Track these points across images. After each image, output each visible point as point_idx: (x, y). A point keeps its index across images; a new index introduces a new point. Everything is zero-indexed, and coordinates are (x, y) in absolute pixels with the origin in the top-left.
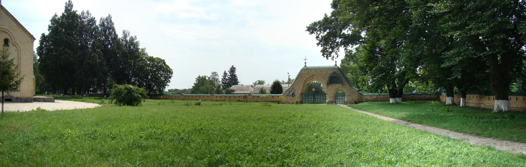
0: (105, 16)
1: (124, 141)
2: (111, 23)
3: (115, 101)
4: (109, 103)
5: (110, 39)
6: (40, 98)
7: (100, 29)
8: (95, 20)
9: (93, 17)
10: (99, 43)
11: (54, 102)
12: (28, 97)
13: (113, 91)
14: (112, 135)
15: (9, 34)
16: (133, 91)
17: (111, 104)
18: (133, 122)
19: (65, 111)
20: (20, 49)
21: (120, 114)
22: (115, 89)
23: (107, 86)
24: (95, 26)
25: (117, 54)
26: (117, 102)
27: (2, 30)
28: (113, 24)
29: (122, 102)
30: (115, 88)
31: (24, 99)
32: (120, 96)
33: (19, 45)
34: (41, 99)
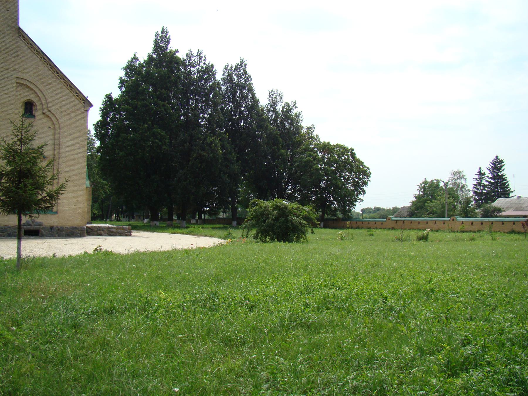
0: (234, 62)
1: (272, 313)
2: (245, 77)
3: (254, 232)
4: (242, 236)
5: (243, 109)
6: (101, 227)
7: (223, 88)
8: (214, 70)
9: (210, 65)
10: (222, 117)
11: (130, 235)
12: (75, 226)
13: (250, 212)
14: (249, 302)
15: (36, 93)
16: (291, 212)
17: (246, 240)
18: (289, 274)
19: (153, 254)
20: (58, 123)
21: (265, 259)
22: (254, 209)
23: (238, 202)
24: (213, 81)
25: (258, 139)
26: (258, 234)
27: (20, 81)
28: (249, 78)
29: (268, 234)
30: (254, 207)
31: (67, 229)
32: (264, 221)
33: (57, 116)
34: (103, 230)
